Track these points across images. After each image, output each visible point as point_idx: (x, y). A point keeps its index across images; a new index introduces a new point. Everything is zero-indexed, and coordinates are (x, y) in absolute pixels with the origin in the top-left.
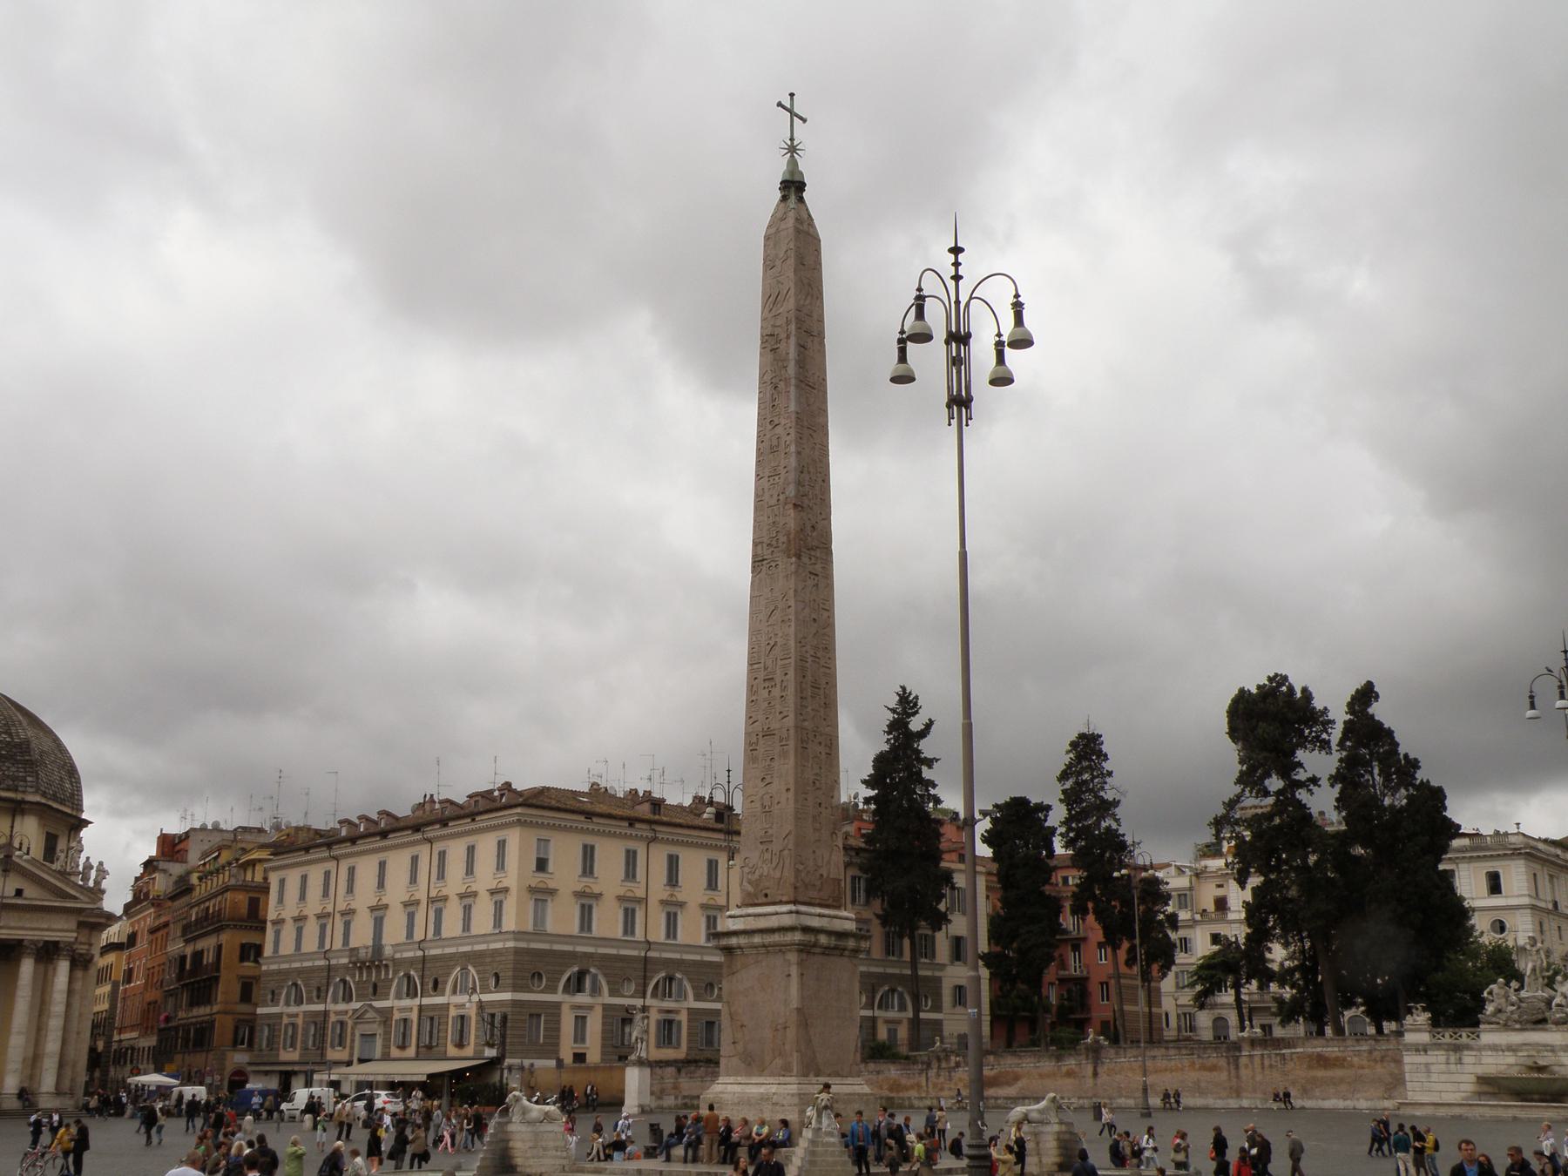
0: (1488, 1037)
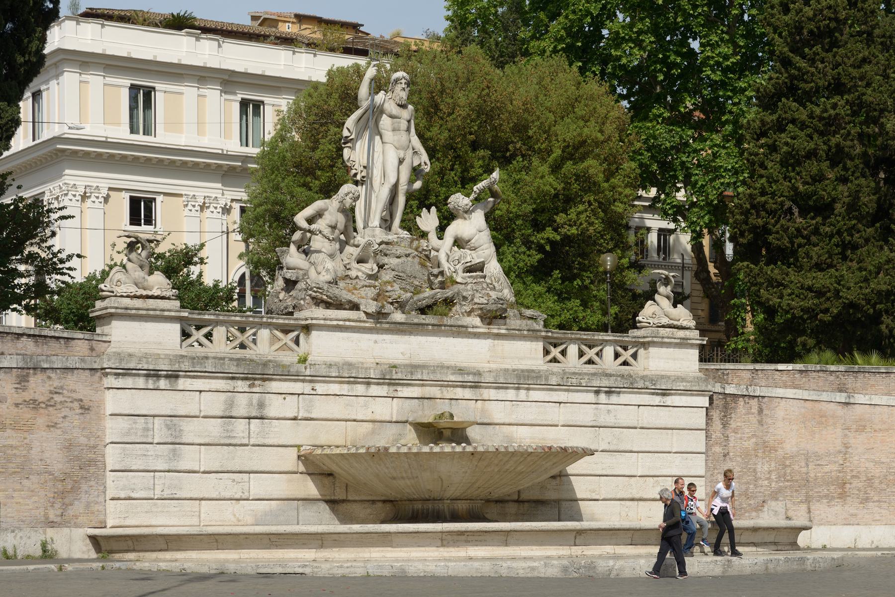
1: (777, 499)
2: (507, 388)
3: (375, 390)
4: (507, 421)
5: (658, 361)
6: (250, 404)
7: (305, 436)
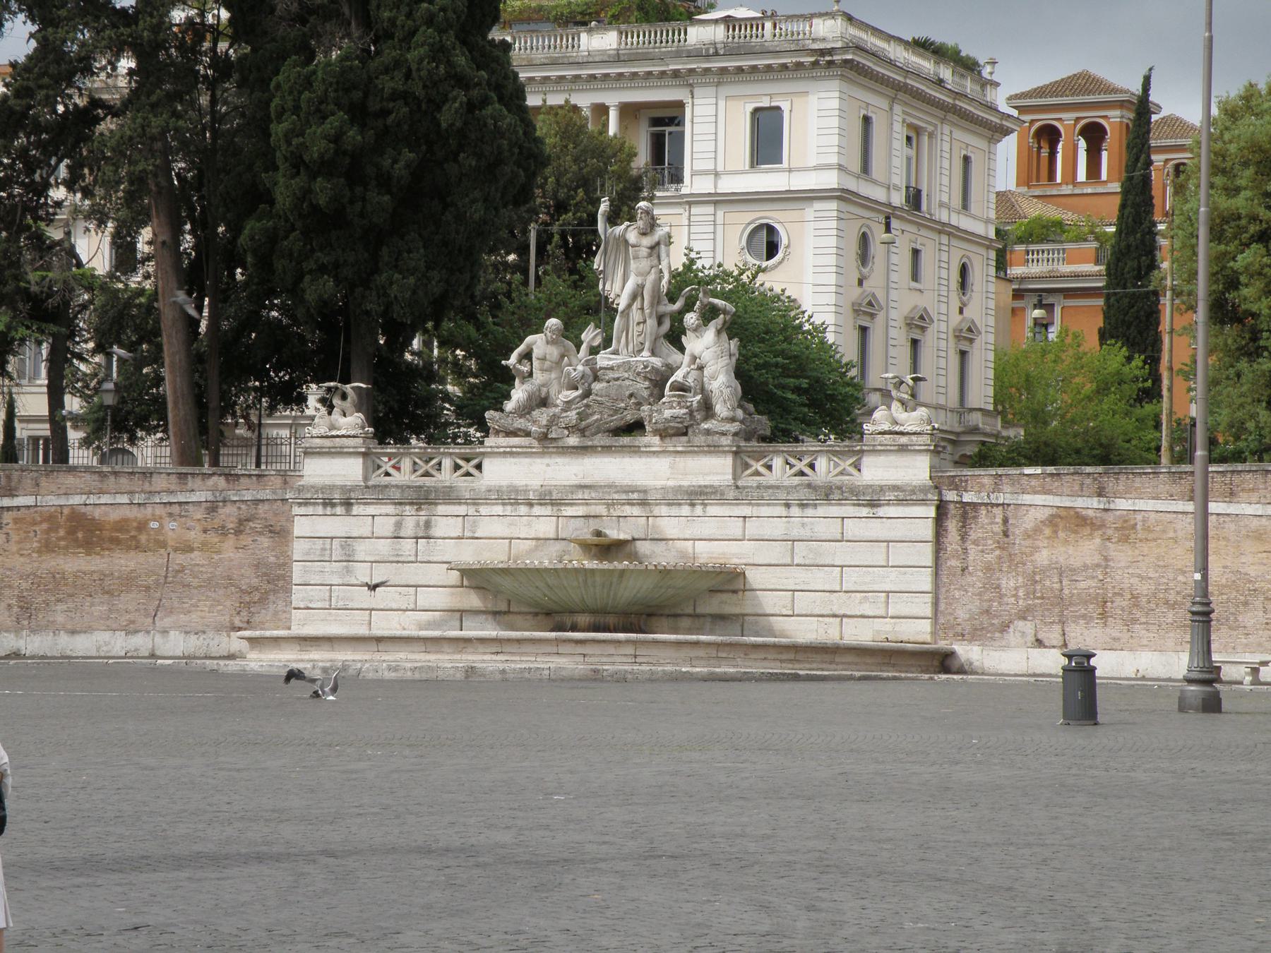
0: (505, 469)
1: (1025, 619)
2: (680, 504)
3: (537, 510)
4: (681, 536)
5: (877, 470)
6: (418, 525)
7: (469, 555)
